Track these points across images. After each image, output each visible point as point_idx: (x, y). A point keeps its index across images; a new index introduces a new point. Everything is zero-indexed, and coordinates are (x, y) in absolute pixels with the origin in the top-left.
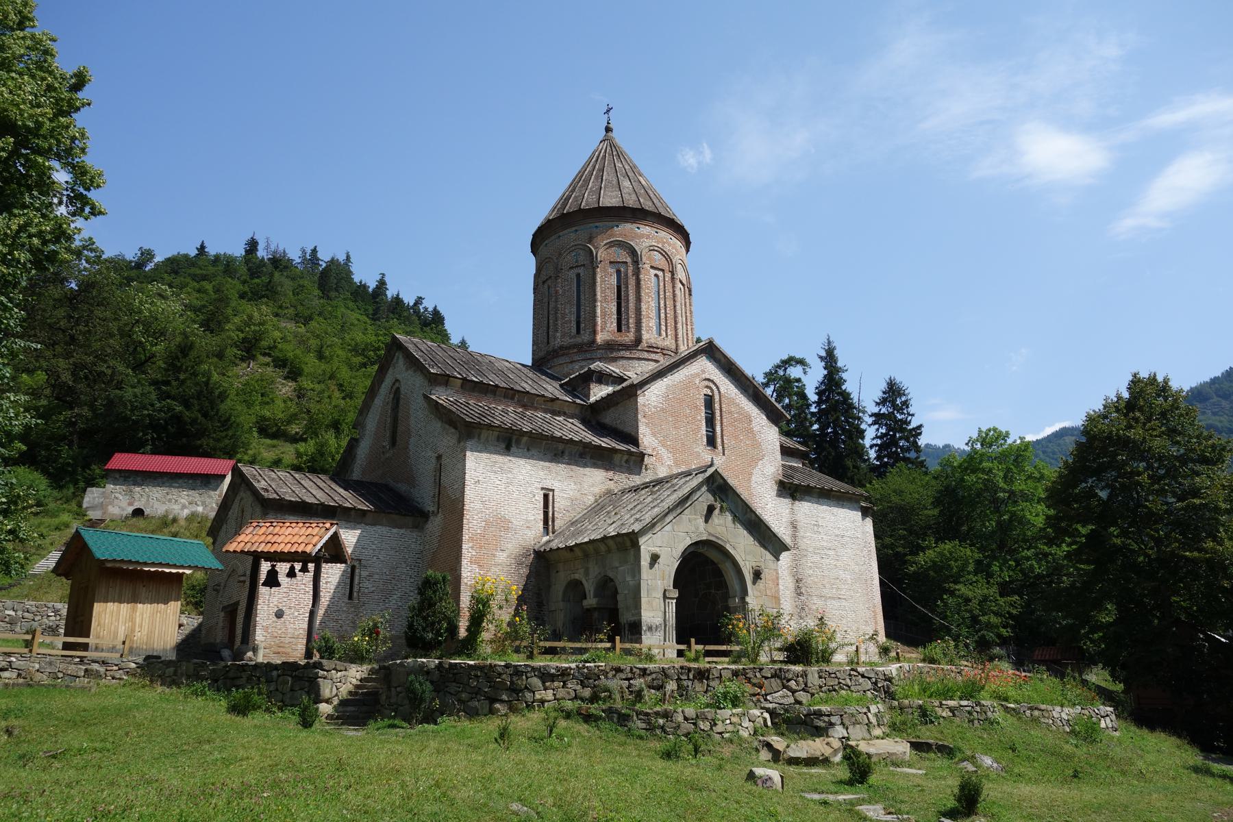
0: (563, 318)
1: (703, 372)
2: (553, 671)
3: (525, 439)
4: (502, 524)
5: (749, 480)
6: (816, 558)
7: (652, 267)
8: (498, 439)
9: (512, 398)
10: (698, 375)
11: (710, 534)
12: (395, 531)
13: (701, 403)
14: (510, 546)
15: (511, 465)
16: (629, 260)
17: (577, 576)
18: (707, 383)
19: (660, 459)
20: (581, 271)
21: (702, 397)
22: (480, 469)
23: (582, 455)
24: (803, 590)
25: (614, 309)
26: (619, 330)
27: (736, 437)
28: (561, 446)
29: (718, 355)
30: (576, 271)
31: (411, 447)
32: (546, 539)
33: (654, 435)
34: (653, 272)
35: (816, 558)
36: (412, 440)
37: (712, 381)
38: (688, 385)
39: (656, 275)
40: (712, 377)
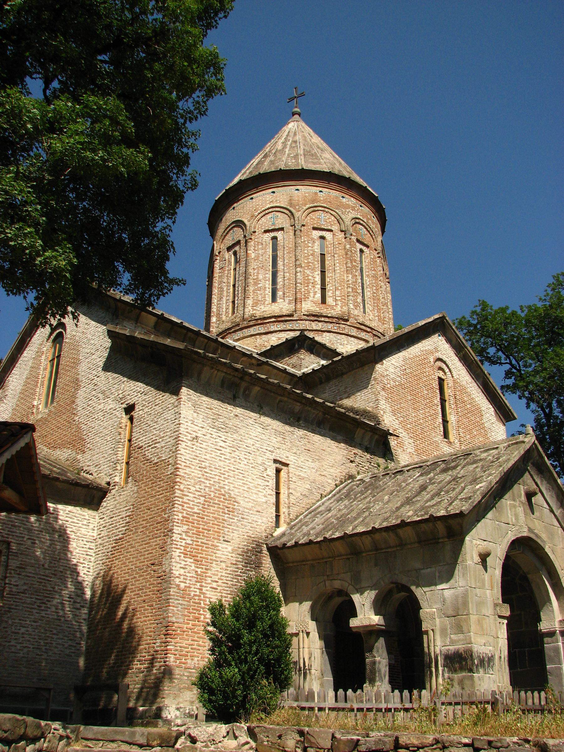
0: (256, 284)
1: (437, 351)
3: (256, 389)
4: (228, 504)
7: (358, 241)
8: (222, 386)
11: (530, 530)
13: (436, 384)
14: (236, 535)
15: (236, 422)
16: (335, 228)
17: (337, 584)
18: (439, 364)
19: (401, 444)
20: (279, 234)
21: (436, 378)
22: (199, 421)
25: (318, 279)
26: (324, 301)
30: (272, 234)
31: (78, 401)
32: (279, 531)
33: (394, 413)
34: (359, 246)
36: (81, 394)
37: (445, 362)
38: (422, 361)
39: (361, 251)
40: (445, 358)
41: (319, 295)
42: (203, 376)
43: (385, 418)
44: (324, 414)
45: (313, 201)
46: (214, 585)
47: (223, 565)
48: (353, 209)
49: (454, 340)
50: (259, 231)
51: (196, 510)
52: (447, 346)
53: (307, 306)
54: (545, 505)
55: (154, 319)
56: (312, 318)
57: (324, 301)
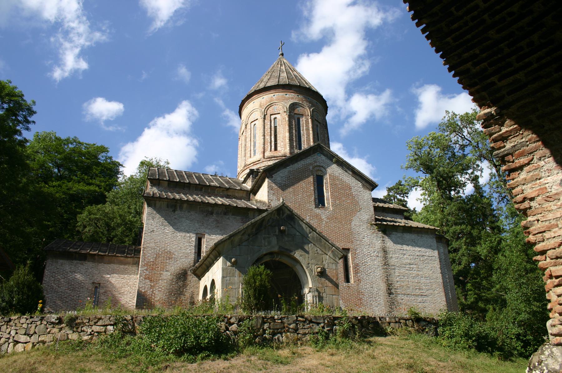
1: (315, 162)
2: (53, 320)
4: (169, 256)
5: (350, 223)
6: (402, 270)
8: (168, 207)
9: (201, 190)
10: (311, 164)
12: (122, 266)
23: (225, 214)
24: (393, 291)
27: (340, 199)
28: (210, 209)
29: (325, 152)
35: (402, 270)
40: (322, 164)
41: (273, 147)
42: (157, 205)
43: (272, 203)
44: (226, 209)
45: (270, 101)
46: (160, 289)
47: (165, 281)
48: (292, 98)
49: (329, 155)
50: (249, 123)
51: (152, 260)
52: (324, 158)
53: (268, 154)
54: (298, 233)
55: (167, 182)
56: (268, 159)
57: (276, 149)
